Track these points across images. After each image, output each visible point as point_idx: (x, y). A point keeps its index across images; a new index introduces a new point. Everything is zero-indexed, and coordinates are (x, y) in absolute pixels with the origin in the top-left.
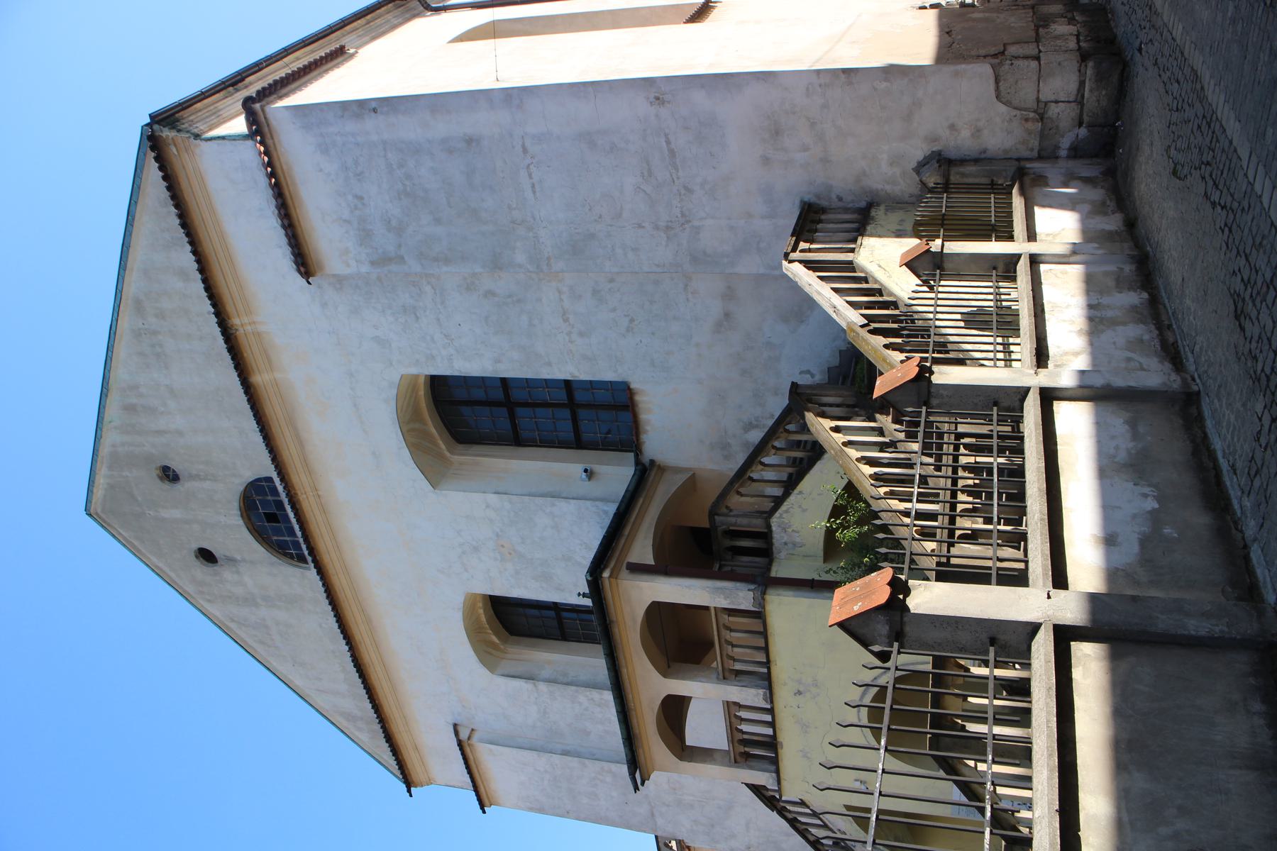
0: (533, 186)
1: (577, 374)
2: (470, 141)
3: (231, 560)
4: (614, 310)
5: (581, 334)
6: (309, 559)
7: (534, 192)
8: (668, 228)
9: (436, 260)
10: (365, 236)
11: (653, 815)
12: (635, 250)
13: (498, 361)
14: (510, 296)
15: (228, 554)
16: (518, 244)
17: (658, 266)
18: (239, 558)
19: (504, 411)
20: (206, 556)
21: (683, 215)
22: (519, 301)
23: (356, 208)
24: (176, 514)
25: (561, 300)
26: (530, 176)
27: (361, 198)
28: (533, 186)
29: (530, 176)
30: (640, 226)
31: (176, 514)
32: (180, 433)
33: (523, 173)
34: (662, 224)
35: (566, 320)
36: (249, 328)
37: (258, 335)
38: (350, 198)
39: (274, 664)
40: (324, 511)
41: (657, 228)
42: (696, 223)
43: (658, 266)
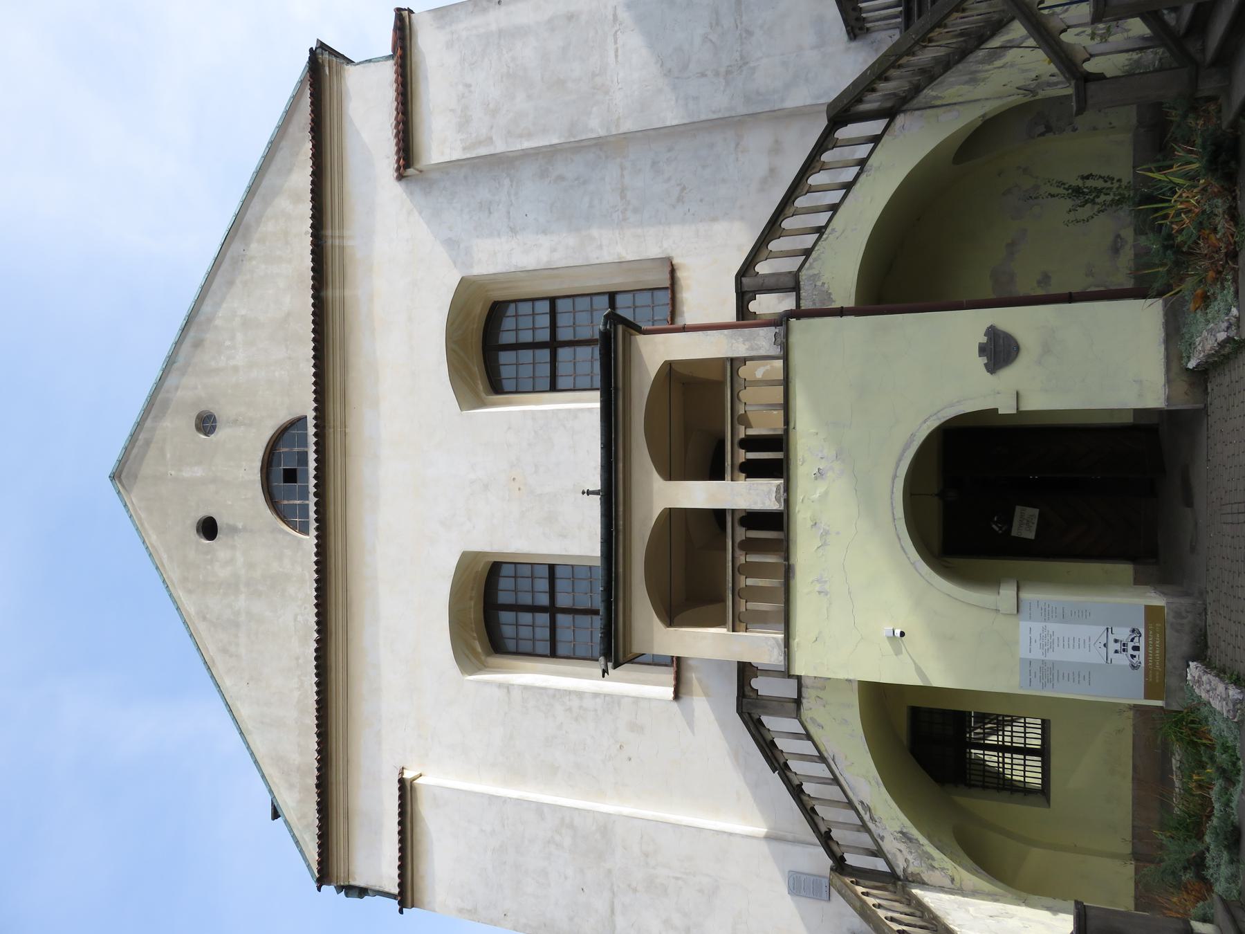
0: (617, 51)
1: (624, 254)
2: (571, 17)
3: (233, 530)
4: (669, 179)
5: (635, 211)
6: (313, 525)
7: (616, 56)
8: (728, 72)
9: (521, 136)
10: (464, 122)
11: (613, 912)
12: (696, 99)
13: (554, 250)
14: (577, 179)
15: (231, 522)
16: (595, 109)
17: (714, 112)
18: (240, 525)
19: (545, 336)
20: (209, 528)
21: (742, 57)
22: (585, 182)
23: (463, 96)
24: (198, 472)
25: (622, 176)
26: (616, 42)
27: (468, 86)
28: (617, 51)
29: (616, 42)
30: (703, 75)
31: (198, 472)
32: (236, 369)
33: (610, 40)
34: (722, 70)
35: (623, 197)
36: (337, 242)
37: (342, 248)
38: (460, 87)
39: (227, 683)
40: (345, 454)
41: (717, 74)
42: (752, 64)
43: (714, 112)
